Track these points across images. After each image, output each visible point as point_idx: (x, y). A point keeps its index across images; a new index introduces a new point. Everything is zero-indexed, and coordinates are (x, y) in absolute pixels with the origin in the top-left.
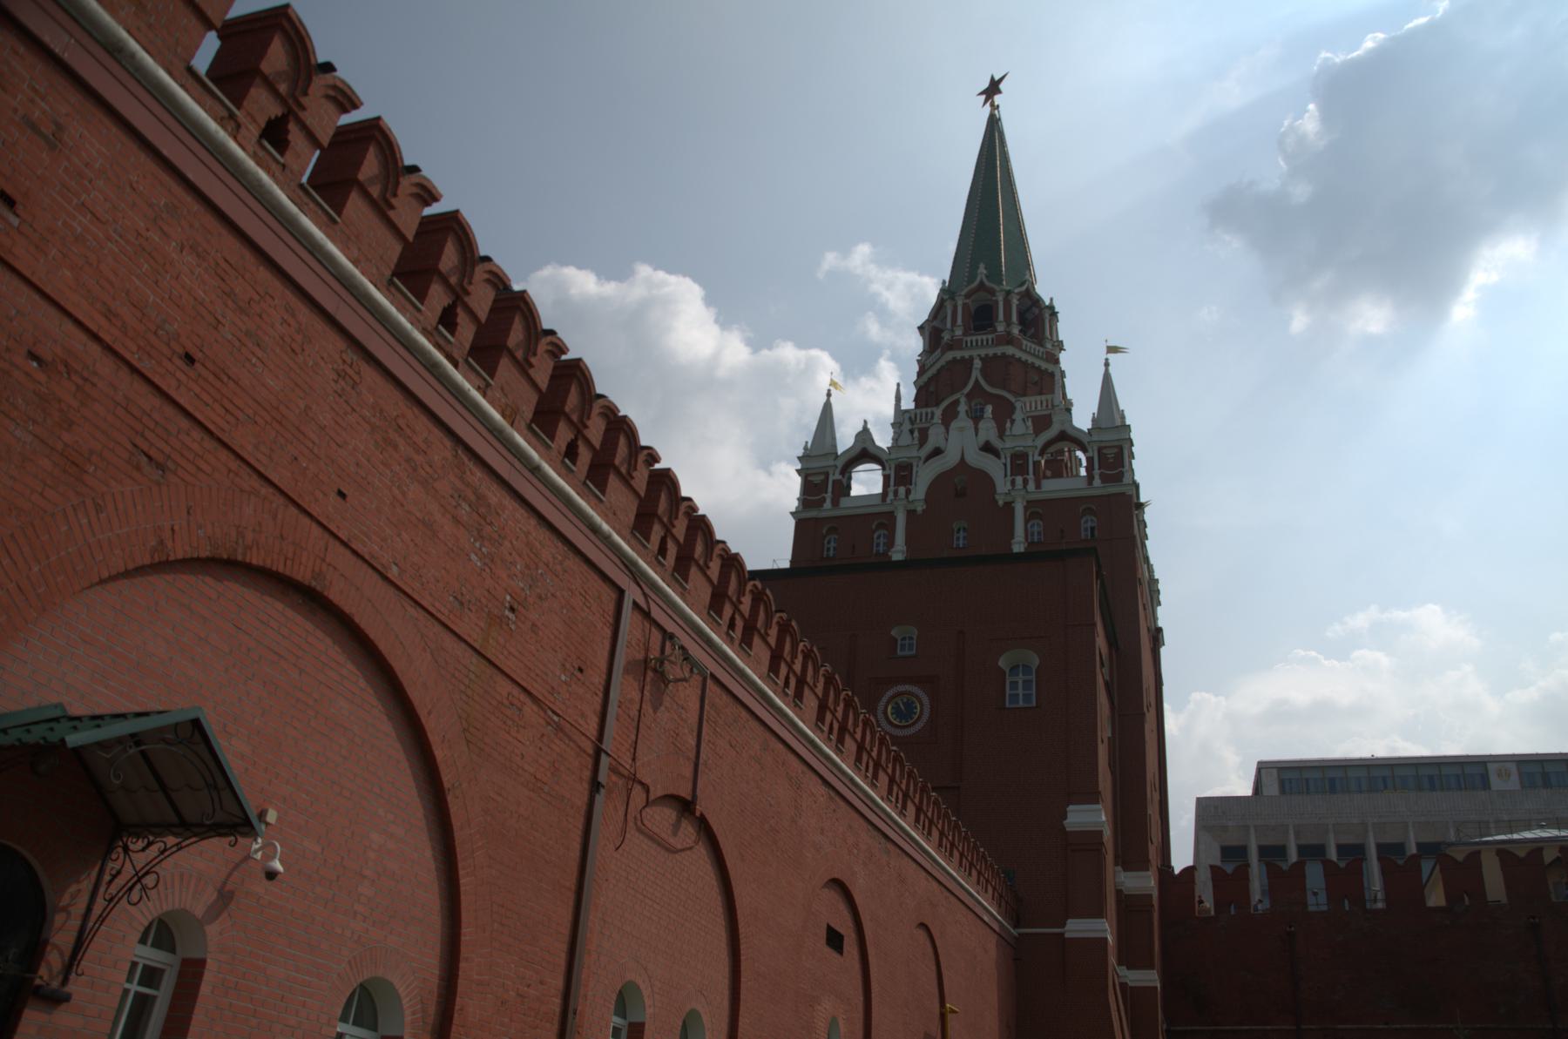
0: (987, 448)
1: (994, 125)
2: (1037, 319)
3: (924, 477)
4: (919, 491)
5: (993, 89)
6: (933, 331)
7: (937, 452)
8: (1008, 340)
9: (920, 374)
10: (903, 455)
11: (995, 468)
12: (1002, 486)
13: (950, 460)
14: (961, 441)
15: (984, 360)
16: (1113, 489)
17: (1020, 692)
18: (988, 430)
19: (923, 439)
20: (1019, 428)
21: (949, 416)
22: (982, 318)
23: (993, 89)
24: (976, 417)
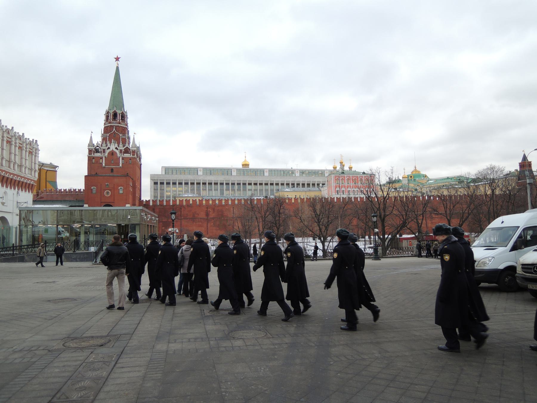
0: (116, 148)
1: (117, 68)
2: (124, 117)
3: (107, 151)
4: (106, 154)
5: (117, 59)
6: (107, 117)
7: (109, 148)
8: (120, 123)
9: (105, 124)
10: (104, 148)
11: (118, 152)
12: (118, 155)
13: (111, 149)
14: (113, 147)
15: (116, 126)
16: (133, 157)
17: (121, 192)
18: (116, 145)
19: (107, 146)
20: (121, 145)
21: (111, 143)
22: (115, 115)
23: (117, 59)
24: (115, 143)
